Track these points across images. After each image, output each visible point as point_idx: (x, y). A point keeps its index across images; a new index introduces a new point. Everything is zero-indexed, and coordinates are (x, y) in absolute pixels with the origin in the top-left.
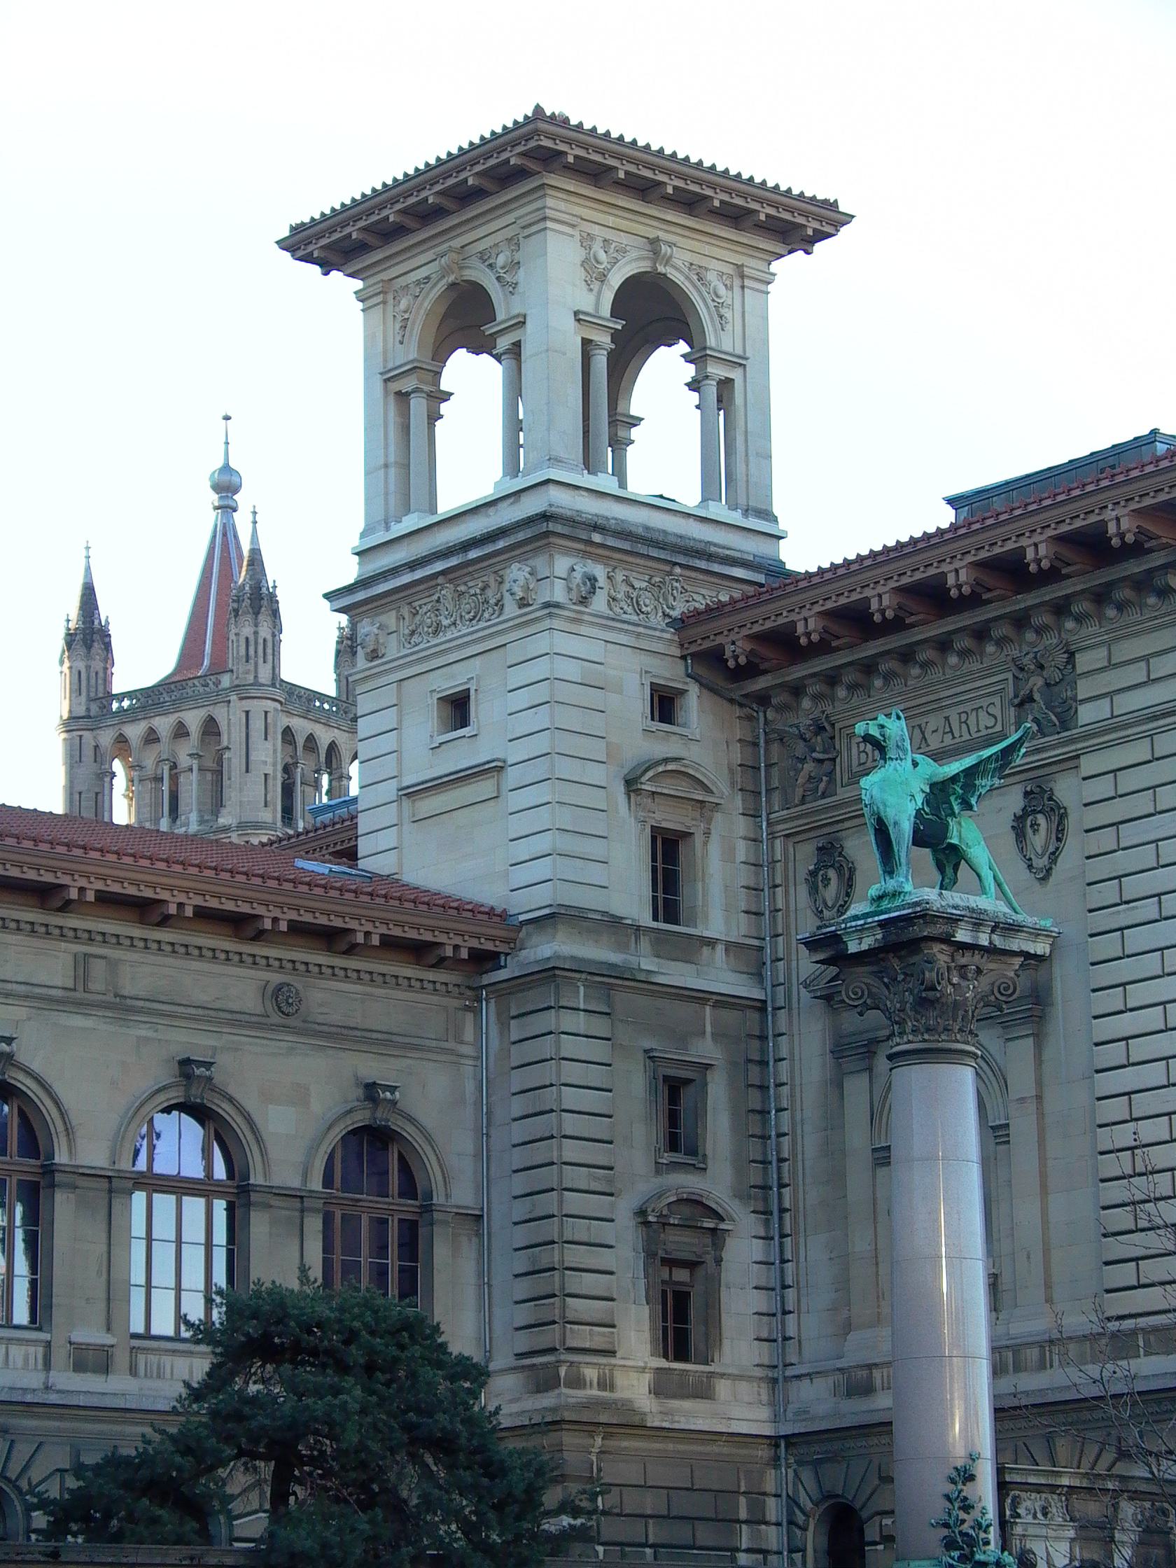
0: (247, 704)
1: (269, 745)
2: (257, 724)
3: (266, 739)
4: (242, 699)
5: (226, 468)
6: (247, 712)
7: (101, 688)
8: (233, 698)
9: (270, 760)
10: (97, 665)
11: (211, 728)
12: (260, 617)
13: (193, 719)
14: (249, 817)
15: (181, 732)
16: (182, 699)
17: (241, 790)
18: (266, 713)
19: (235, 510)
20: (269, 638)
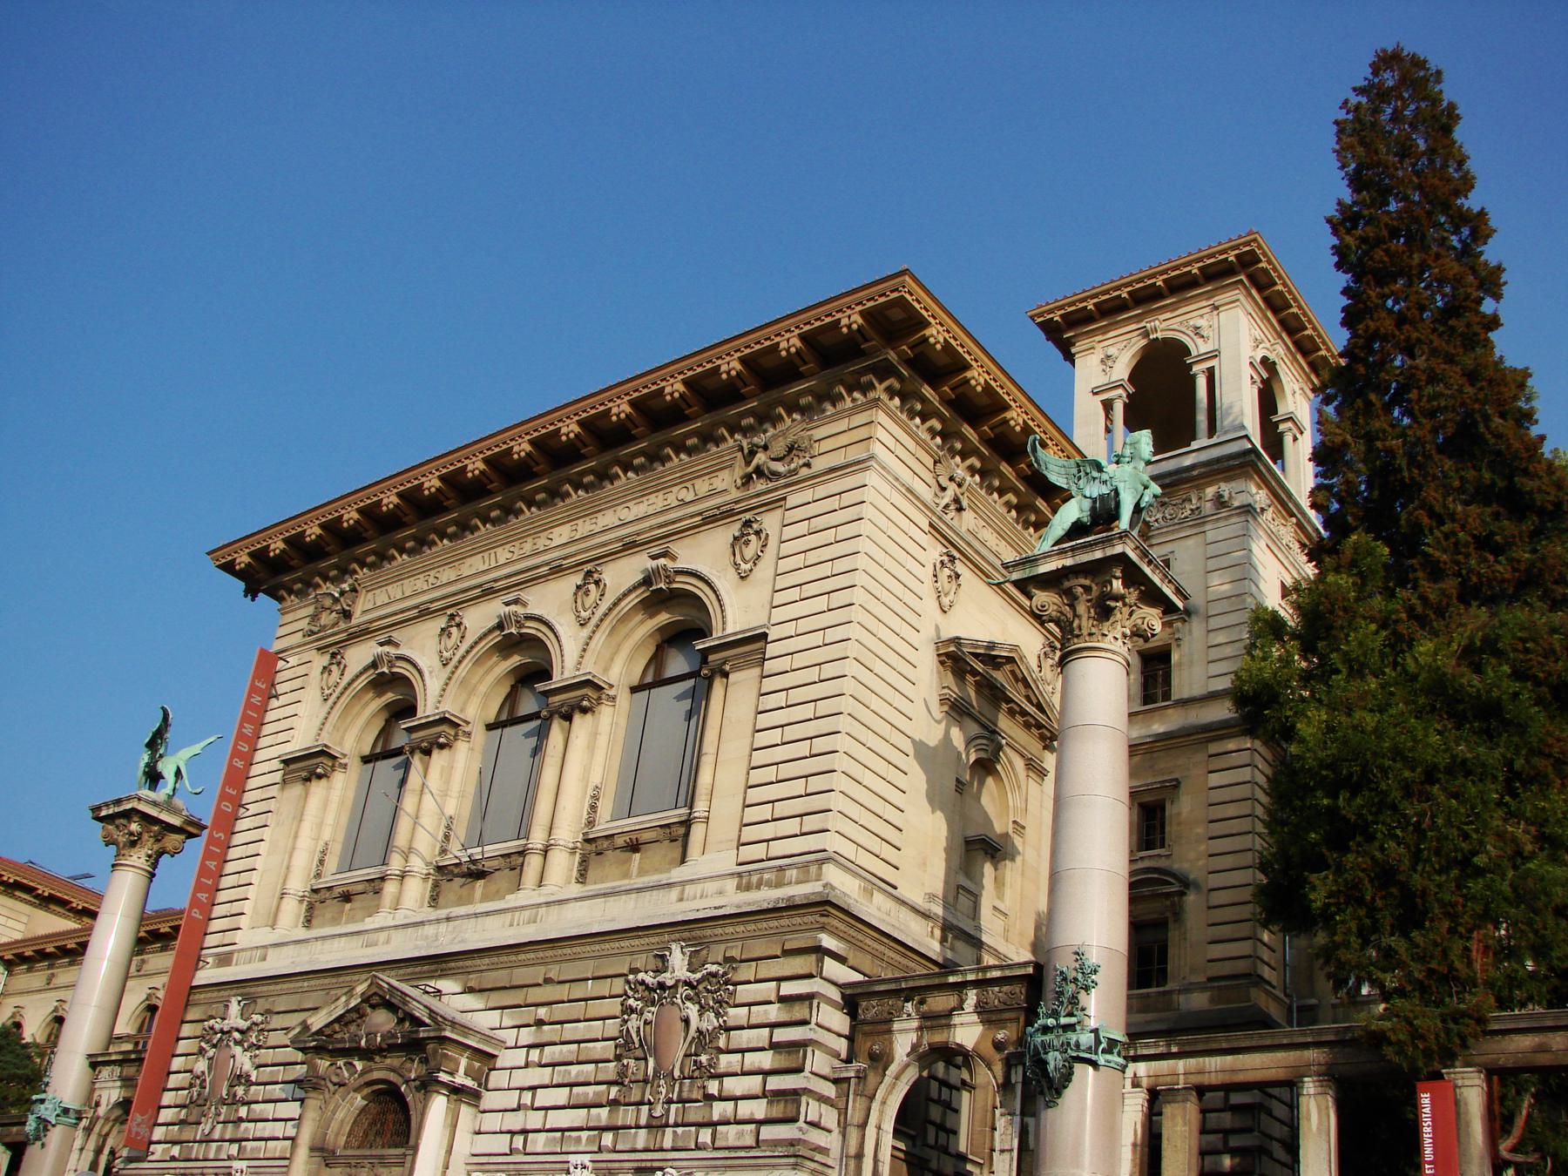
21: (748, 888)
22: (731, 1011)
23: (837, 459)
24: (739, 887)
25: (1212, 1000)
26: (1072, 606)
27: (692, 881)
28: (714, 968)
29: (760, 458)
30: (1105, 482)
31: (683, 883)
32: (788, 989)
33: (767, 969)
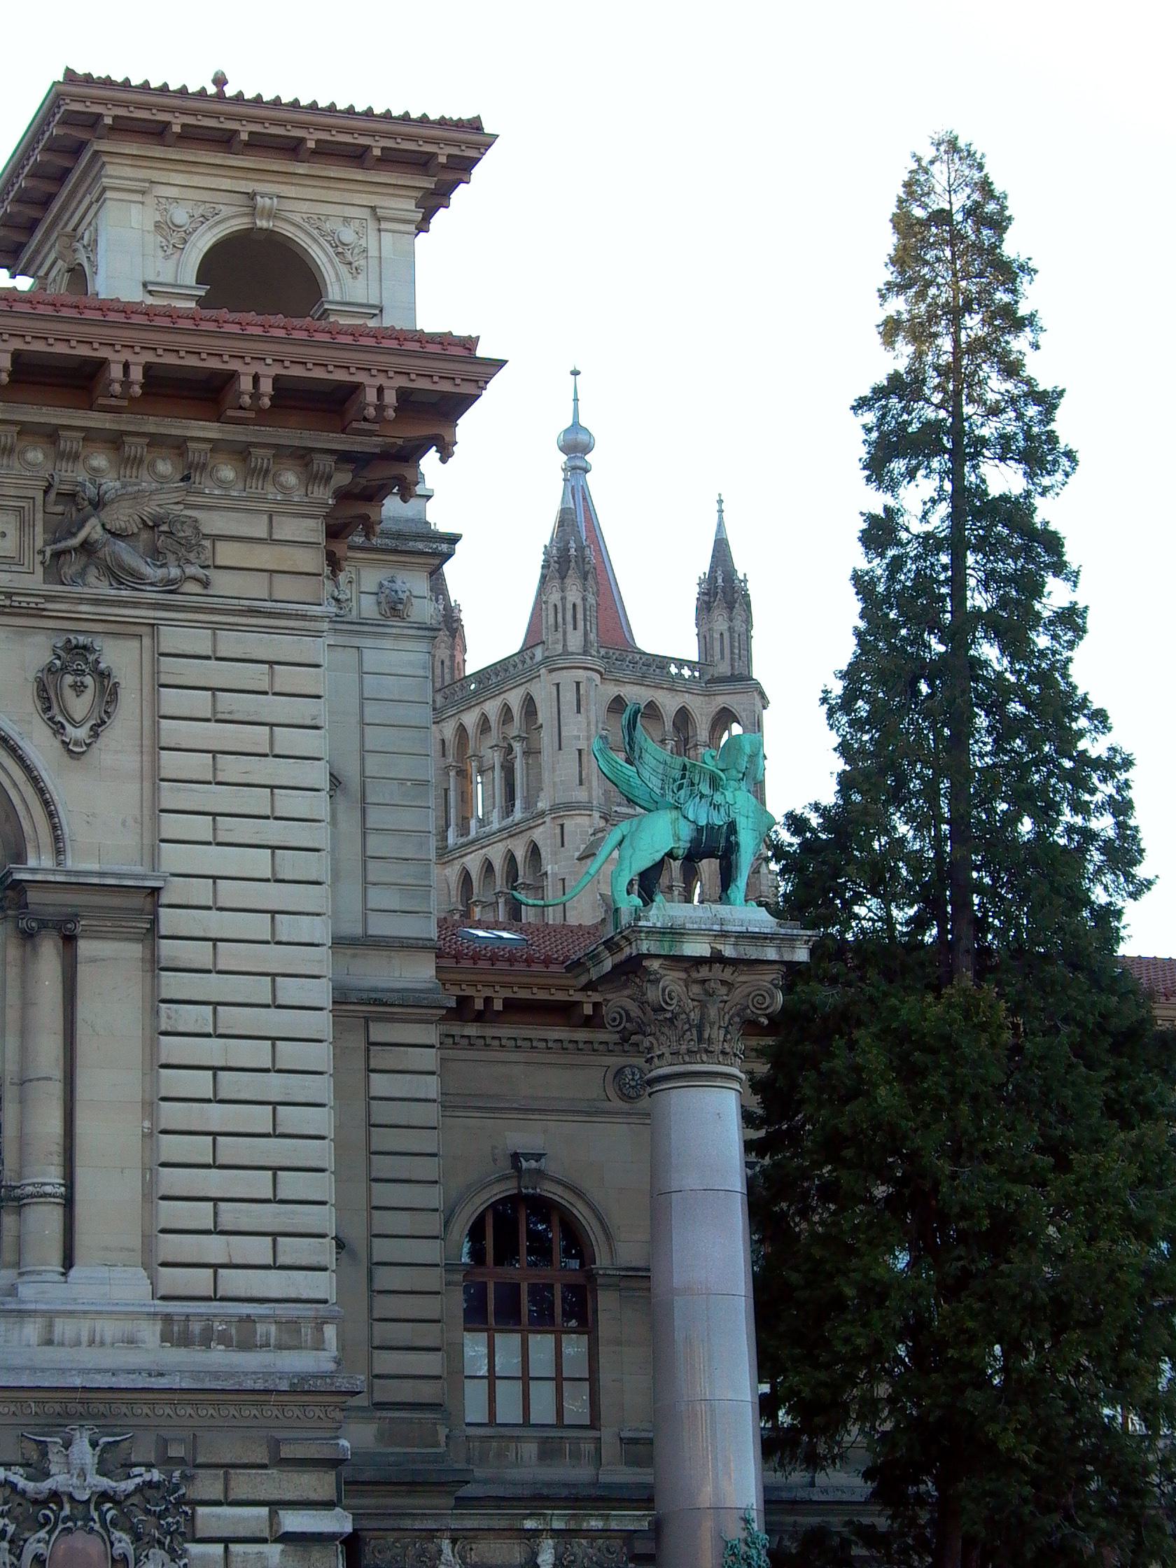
0: (557, 677)
1: (581, 718)
2: (569, 696)
3: (579, 711)
4: (551, 671)
5: (576, 426)
6: (558, 685)
7: (447, 677)
8: (543, 671)
9: (583, 734)
10: (443, 653)
11: (530, 706)
12: (568, 581)
13: (514, 699)
14: (561, 798)
15: (507, 710)
16: (504, 681)
17: (554, 770)
18: (578, 684)
19: (586, 471)
20: (579, 602)
21: (184, 1341)
22: (194, 1549)
23: (254, 587)
24: (165, 1337)
25: (381, 1437)
26: (703, 1005)
27: (71, 1314)
28: (156, 1475)
29: (92, 530)
30: (717, 807)
31: (50, 1316)
32: (293, 1521)
33: (243, 1485)
